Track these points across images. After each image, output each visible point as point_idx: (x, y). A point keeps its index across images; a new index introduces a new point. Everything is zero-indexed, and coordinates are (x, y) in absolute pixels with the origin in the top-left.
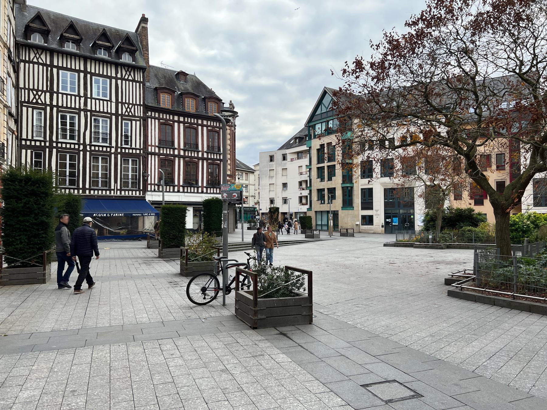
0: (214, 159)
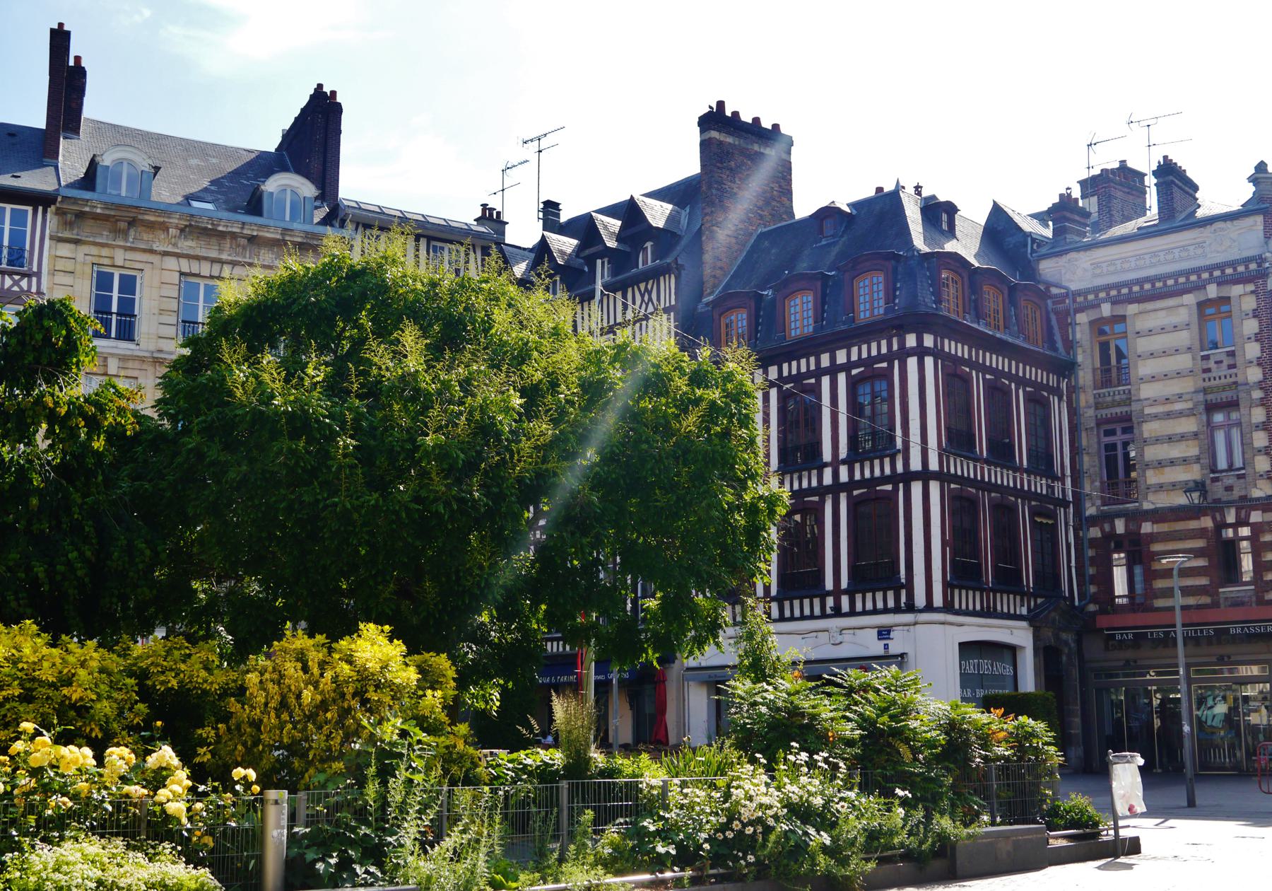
0: (873, 478)
